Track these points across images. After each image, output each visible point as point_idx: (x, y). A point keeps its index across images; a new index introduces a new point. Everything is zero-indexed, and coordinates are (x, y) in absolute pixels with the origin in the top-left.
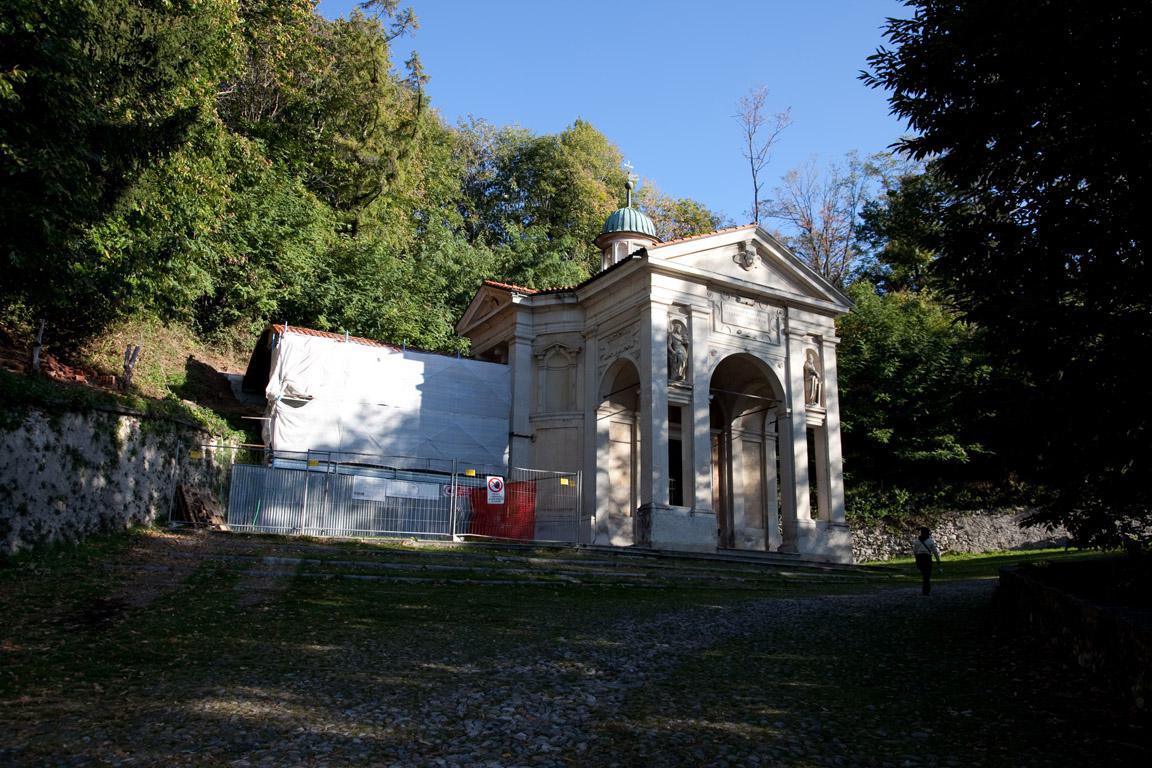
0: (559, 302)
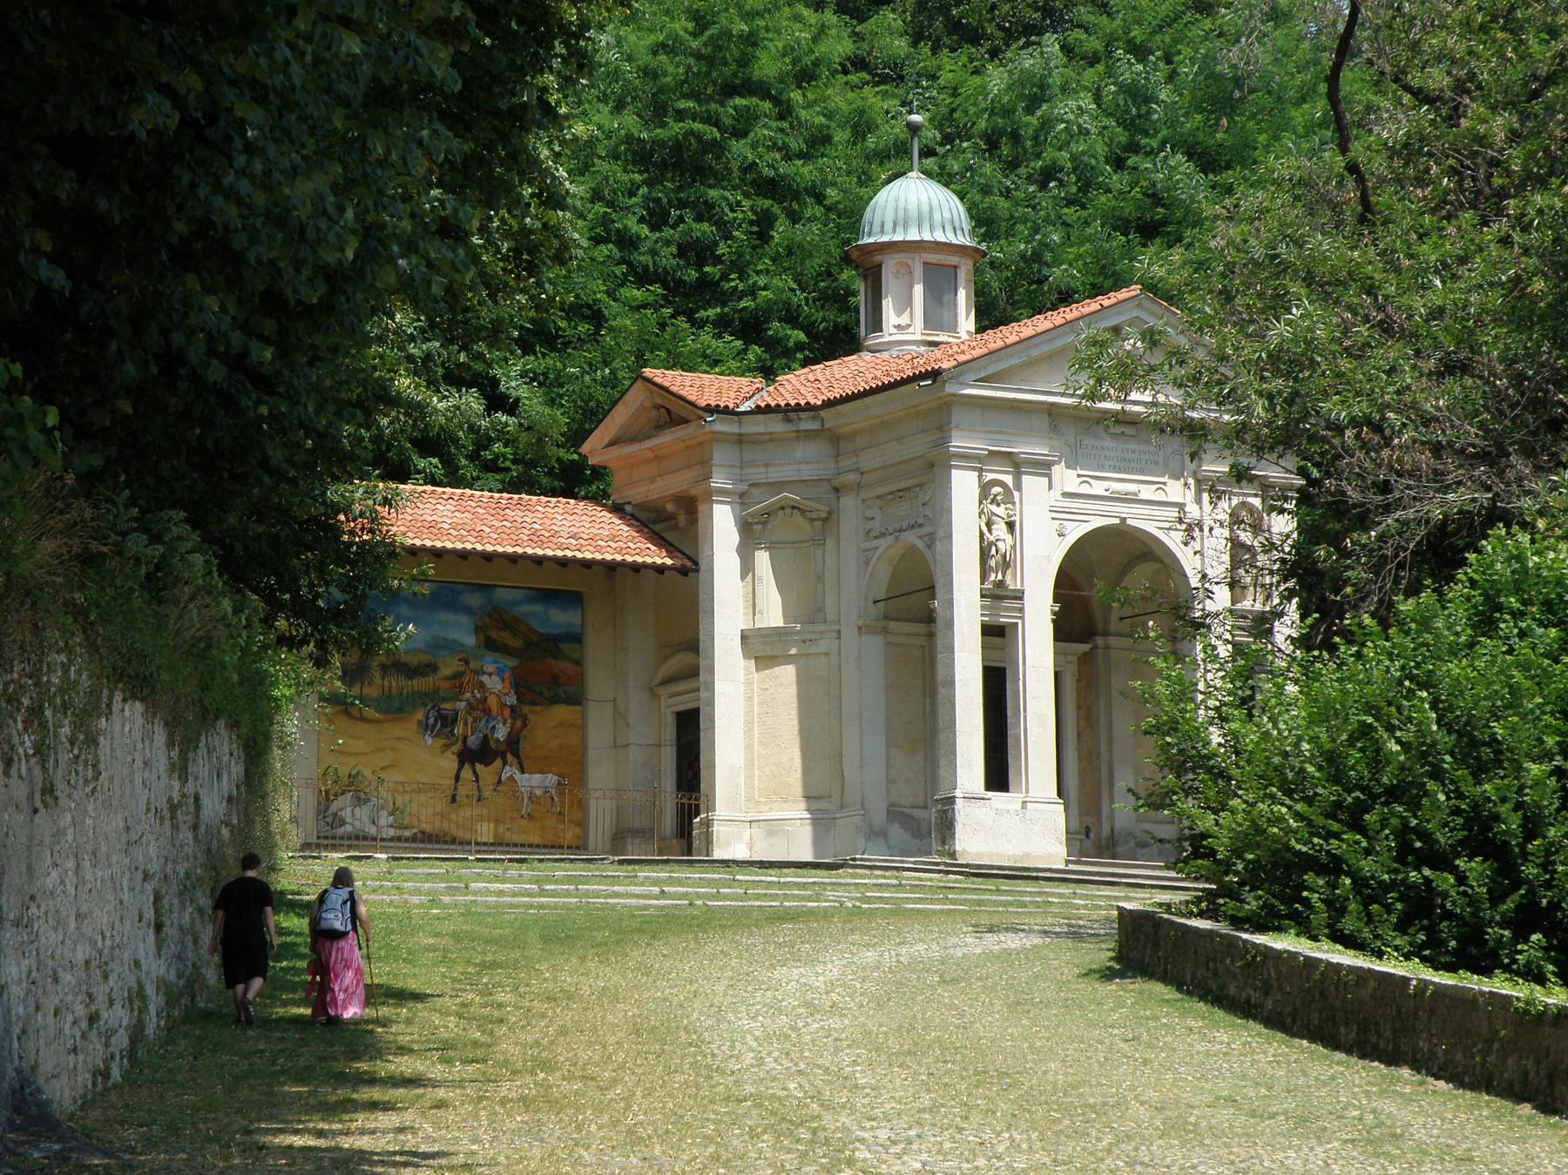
0: (791, 427)
